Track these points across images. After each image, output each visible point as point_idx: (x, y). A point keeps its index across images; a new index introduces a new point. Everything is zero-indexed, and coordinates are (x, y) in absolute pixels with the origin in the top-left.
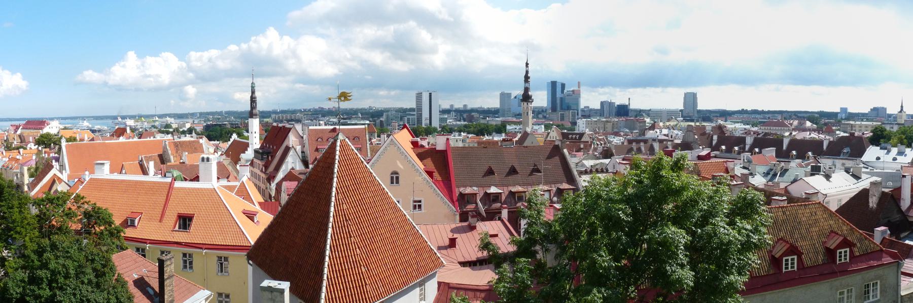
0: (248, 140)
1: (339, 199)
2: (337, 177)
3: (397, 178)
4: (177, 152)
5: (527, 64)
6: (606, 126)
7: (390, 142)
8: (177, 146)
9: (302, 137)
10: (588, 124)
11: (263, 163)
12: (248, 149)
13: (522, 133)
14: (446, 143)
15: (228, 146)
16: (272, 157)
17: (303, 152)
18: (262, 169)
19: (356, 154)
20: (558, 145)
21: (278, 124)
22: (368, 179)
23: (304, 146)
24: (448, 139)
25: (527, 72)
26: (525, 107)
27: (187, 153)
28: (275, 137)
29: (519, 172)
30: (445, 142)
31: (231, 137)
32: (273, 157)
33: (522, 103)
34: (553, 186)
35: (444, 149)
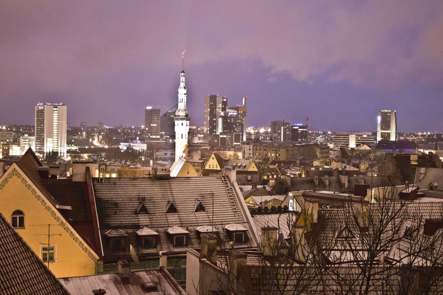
3: (22, 220)
7: (13, 171)
10: (256, 150)
14: (86, 174)
30: (84, 172)
35: (85, 181)
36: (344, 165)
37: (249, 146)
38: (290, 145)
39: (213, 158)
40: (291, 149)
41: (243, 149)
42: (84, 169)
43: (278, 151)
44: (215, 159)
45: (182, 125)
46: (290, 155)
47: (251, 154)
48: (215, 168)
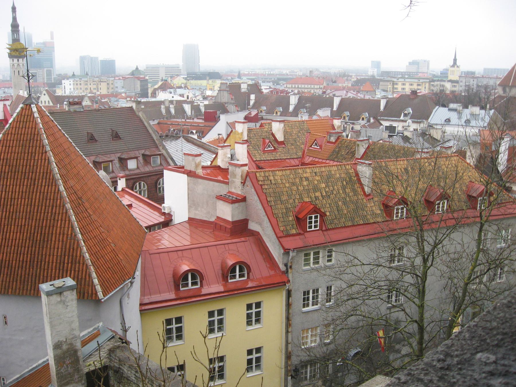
1: (63, 176)
2: (51, 150)
5: (14, 9)
6: (100, 87)
10: (77, 84)
13: (14, 98)
19: (52, 121)
20: (132, 107)
22: (71, 148)
24: (5, 105)
25: (14, 19)
26: (16, 65)
29: (97, 139)
30: (2, 109)
33: (11, 60)
34: (137, 152)
35: (3, 118)
36: (172, 95)
37: (68, 81)
38: (110, 79)
39: (45, 95)
40: (111, 82)
41: (63, 85)
42: (2, 106)
43: (99, 84)
44: (46, 94)
45: (18, 61)
46: (110, 88)
47: (72, 90)
48: (47, 104)
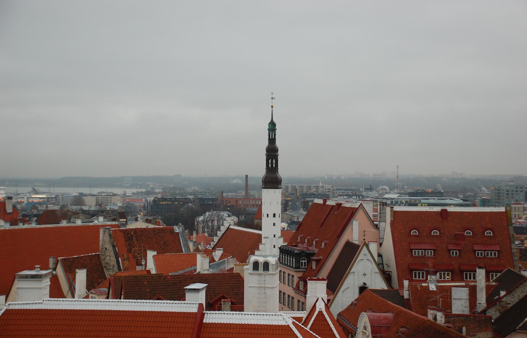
0: (261, 230)
4: (129, 251)
8: (131, 238)
9: (377, 227)
11: (300, 275)
12: (261, 246)
15: (216, 239)
16: (318, 261)
17: (380, 255)
18: (298, 284)
21: (325, 201)
23: (381, 244)
27: (155, 253)
28: (321, 226)
31: (223, 225)
32: (320, 264)
